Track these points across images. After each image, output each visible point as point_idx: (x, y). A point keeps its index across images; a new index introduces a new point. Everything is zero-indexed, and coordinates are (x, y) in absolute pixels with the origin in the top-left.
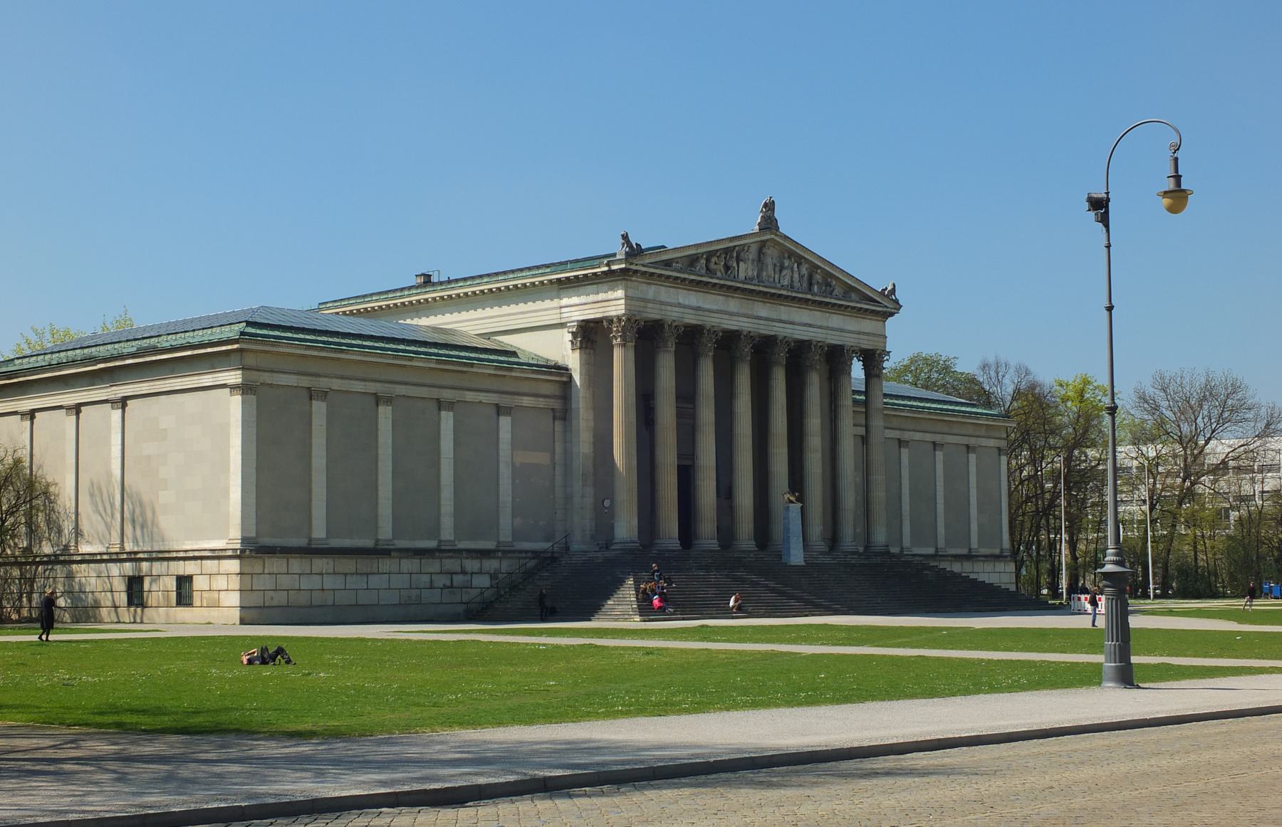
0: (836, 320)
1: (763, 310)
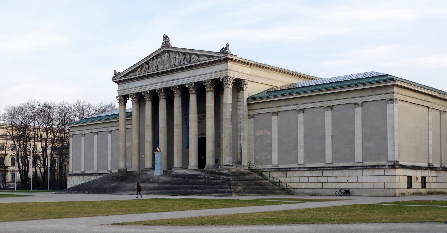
1: (166, 78)
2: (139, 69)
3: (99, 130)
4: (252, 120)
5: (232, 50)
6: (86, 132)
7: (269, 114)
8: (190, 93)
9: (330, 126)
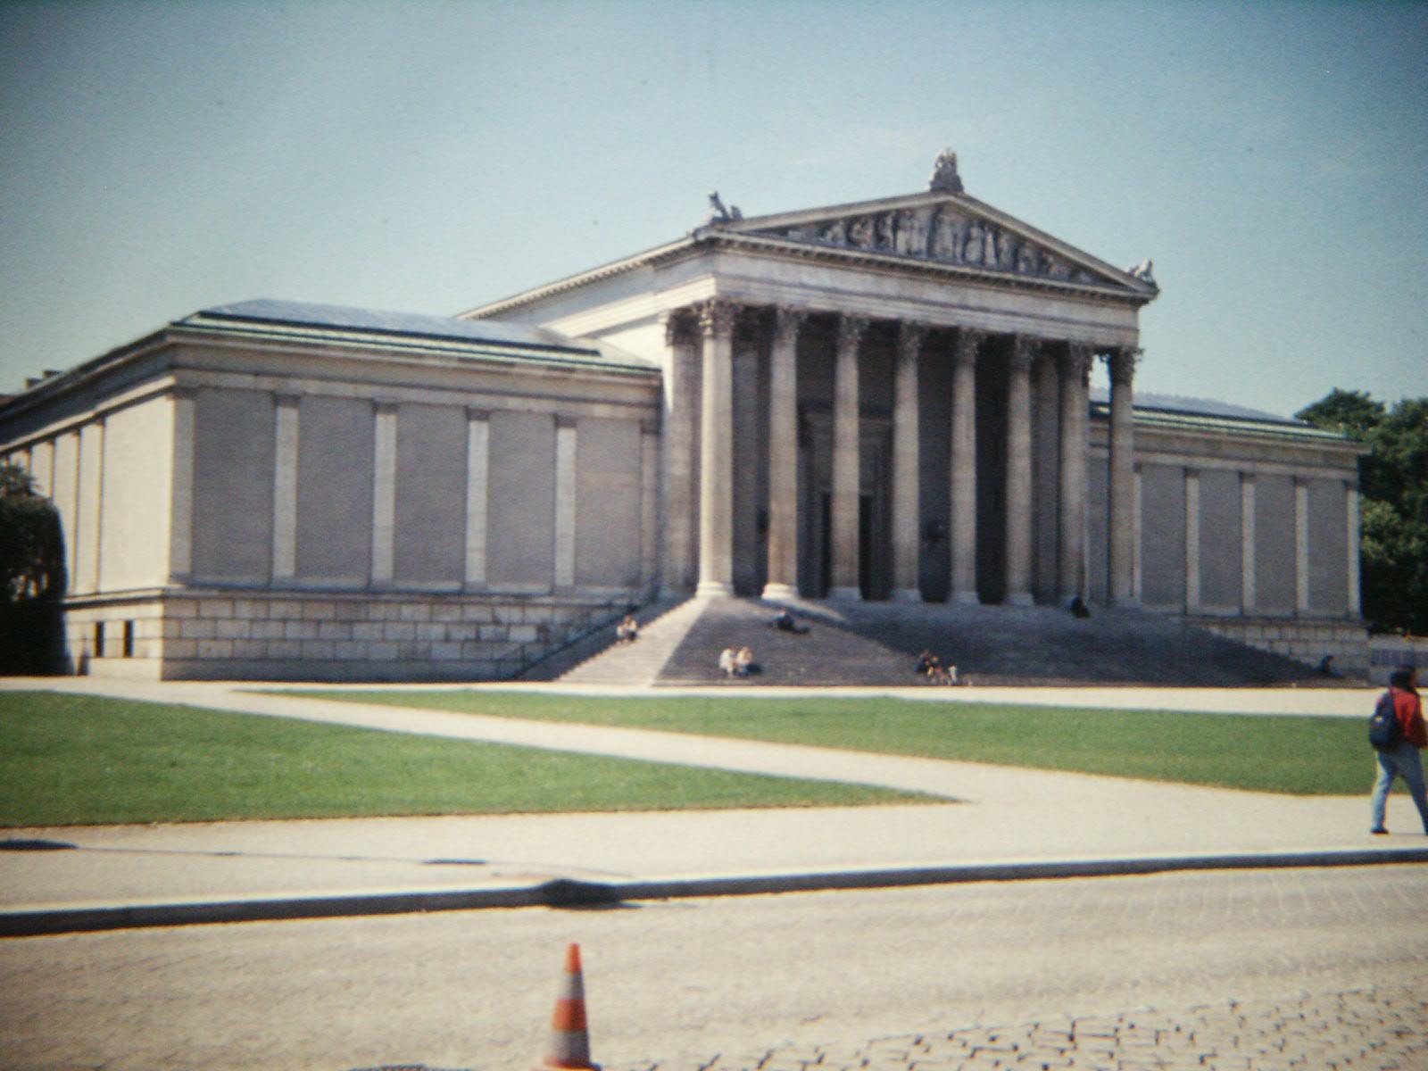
0: (1056, 308)
6: (313, 387)
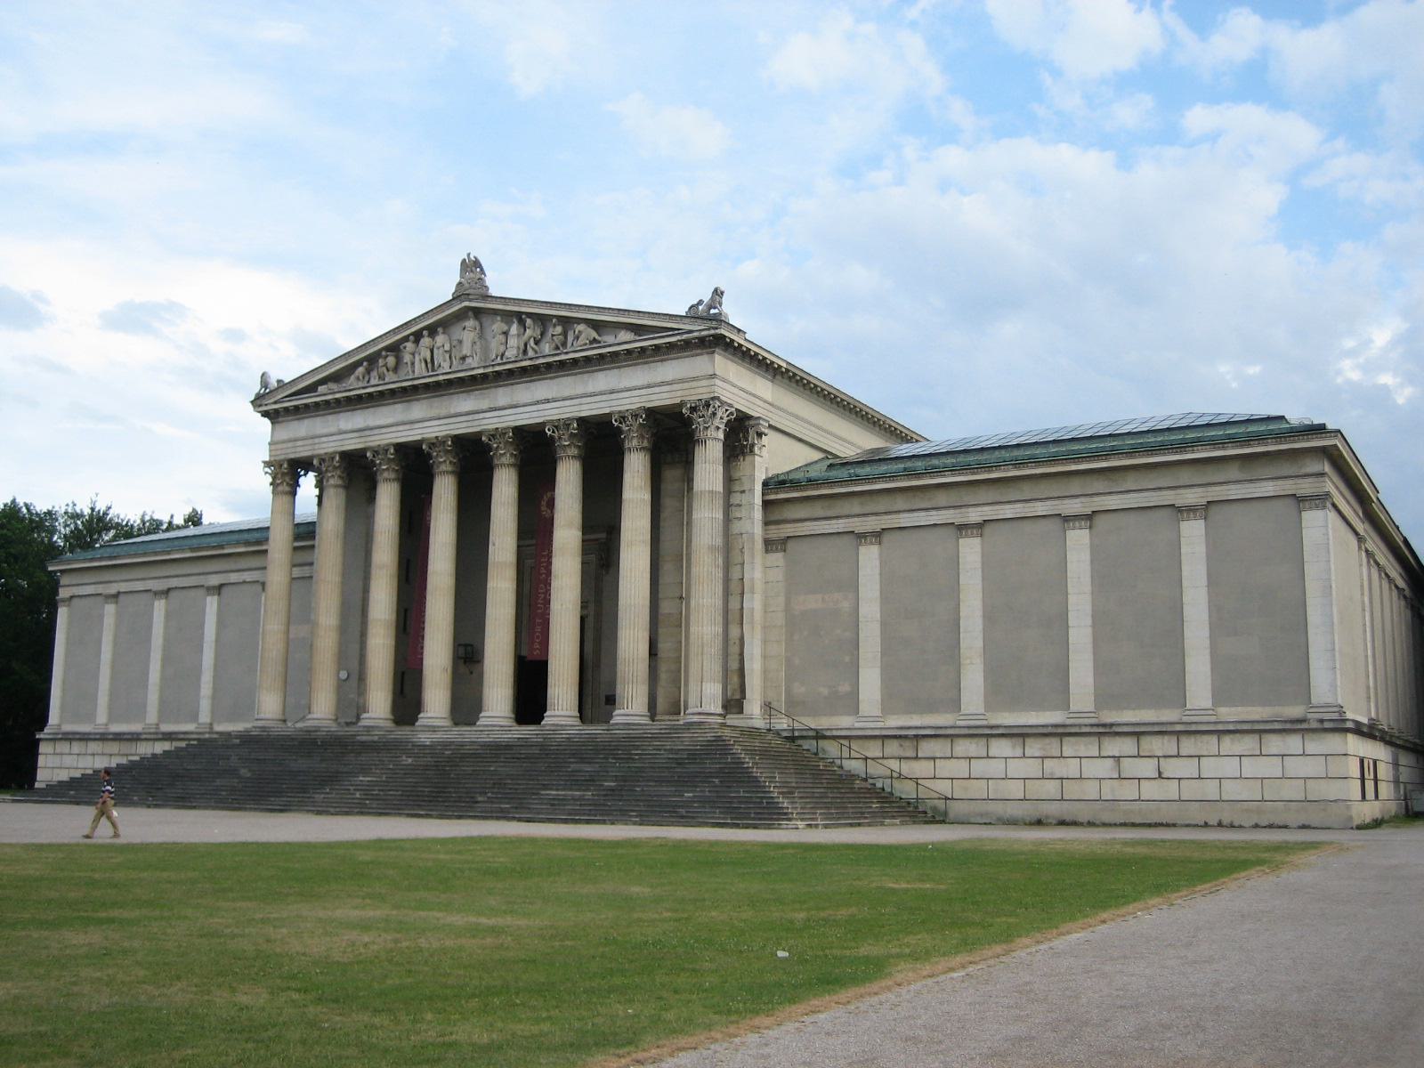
0: (602, 380)
1: (464, 403)
2: (361, 370)
3: (174, 583)
4: (777, 558)
5: (734, 312)
6: (123, 587)
7: (846, 538)
8: (561, 453)
9: (1086, 580)
